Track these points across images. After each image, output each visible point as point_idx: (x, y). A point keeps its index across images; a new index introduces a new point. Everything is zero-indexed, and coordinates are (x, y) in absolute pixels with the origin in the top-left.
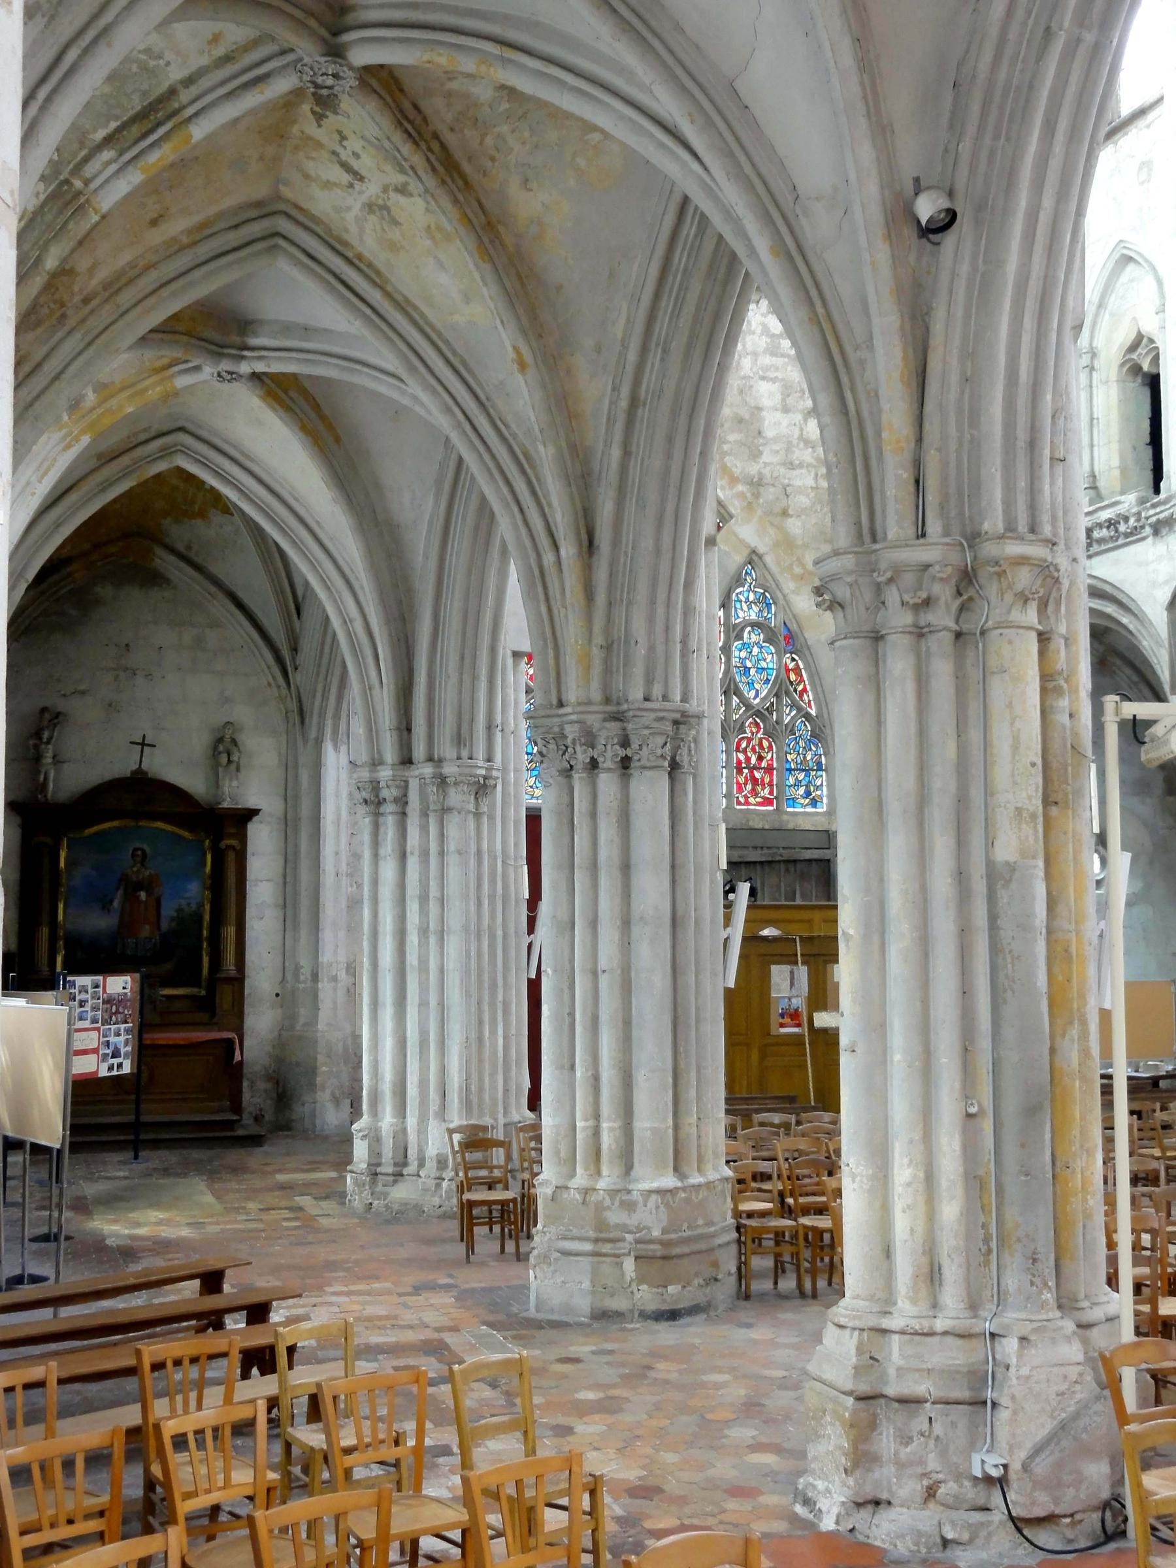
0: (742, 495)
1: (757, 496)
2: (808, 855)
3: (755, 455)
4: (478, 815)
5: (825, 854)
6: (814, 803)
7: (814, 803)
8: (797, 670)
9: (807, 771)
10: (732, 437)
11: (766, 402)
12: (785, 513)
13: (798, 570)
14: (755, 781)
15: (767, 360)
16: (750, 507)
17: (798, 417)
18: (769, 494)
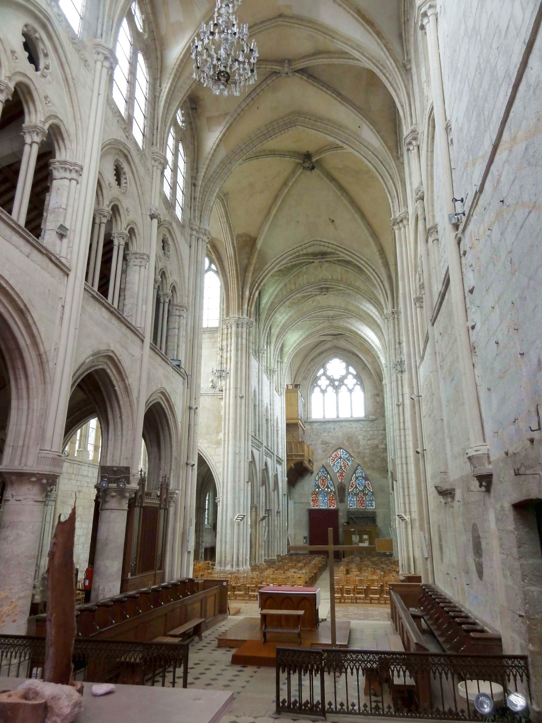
3: (358, 448)
11: (360, 439)
12: (364, 457)
15: (360, 432)
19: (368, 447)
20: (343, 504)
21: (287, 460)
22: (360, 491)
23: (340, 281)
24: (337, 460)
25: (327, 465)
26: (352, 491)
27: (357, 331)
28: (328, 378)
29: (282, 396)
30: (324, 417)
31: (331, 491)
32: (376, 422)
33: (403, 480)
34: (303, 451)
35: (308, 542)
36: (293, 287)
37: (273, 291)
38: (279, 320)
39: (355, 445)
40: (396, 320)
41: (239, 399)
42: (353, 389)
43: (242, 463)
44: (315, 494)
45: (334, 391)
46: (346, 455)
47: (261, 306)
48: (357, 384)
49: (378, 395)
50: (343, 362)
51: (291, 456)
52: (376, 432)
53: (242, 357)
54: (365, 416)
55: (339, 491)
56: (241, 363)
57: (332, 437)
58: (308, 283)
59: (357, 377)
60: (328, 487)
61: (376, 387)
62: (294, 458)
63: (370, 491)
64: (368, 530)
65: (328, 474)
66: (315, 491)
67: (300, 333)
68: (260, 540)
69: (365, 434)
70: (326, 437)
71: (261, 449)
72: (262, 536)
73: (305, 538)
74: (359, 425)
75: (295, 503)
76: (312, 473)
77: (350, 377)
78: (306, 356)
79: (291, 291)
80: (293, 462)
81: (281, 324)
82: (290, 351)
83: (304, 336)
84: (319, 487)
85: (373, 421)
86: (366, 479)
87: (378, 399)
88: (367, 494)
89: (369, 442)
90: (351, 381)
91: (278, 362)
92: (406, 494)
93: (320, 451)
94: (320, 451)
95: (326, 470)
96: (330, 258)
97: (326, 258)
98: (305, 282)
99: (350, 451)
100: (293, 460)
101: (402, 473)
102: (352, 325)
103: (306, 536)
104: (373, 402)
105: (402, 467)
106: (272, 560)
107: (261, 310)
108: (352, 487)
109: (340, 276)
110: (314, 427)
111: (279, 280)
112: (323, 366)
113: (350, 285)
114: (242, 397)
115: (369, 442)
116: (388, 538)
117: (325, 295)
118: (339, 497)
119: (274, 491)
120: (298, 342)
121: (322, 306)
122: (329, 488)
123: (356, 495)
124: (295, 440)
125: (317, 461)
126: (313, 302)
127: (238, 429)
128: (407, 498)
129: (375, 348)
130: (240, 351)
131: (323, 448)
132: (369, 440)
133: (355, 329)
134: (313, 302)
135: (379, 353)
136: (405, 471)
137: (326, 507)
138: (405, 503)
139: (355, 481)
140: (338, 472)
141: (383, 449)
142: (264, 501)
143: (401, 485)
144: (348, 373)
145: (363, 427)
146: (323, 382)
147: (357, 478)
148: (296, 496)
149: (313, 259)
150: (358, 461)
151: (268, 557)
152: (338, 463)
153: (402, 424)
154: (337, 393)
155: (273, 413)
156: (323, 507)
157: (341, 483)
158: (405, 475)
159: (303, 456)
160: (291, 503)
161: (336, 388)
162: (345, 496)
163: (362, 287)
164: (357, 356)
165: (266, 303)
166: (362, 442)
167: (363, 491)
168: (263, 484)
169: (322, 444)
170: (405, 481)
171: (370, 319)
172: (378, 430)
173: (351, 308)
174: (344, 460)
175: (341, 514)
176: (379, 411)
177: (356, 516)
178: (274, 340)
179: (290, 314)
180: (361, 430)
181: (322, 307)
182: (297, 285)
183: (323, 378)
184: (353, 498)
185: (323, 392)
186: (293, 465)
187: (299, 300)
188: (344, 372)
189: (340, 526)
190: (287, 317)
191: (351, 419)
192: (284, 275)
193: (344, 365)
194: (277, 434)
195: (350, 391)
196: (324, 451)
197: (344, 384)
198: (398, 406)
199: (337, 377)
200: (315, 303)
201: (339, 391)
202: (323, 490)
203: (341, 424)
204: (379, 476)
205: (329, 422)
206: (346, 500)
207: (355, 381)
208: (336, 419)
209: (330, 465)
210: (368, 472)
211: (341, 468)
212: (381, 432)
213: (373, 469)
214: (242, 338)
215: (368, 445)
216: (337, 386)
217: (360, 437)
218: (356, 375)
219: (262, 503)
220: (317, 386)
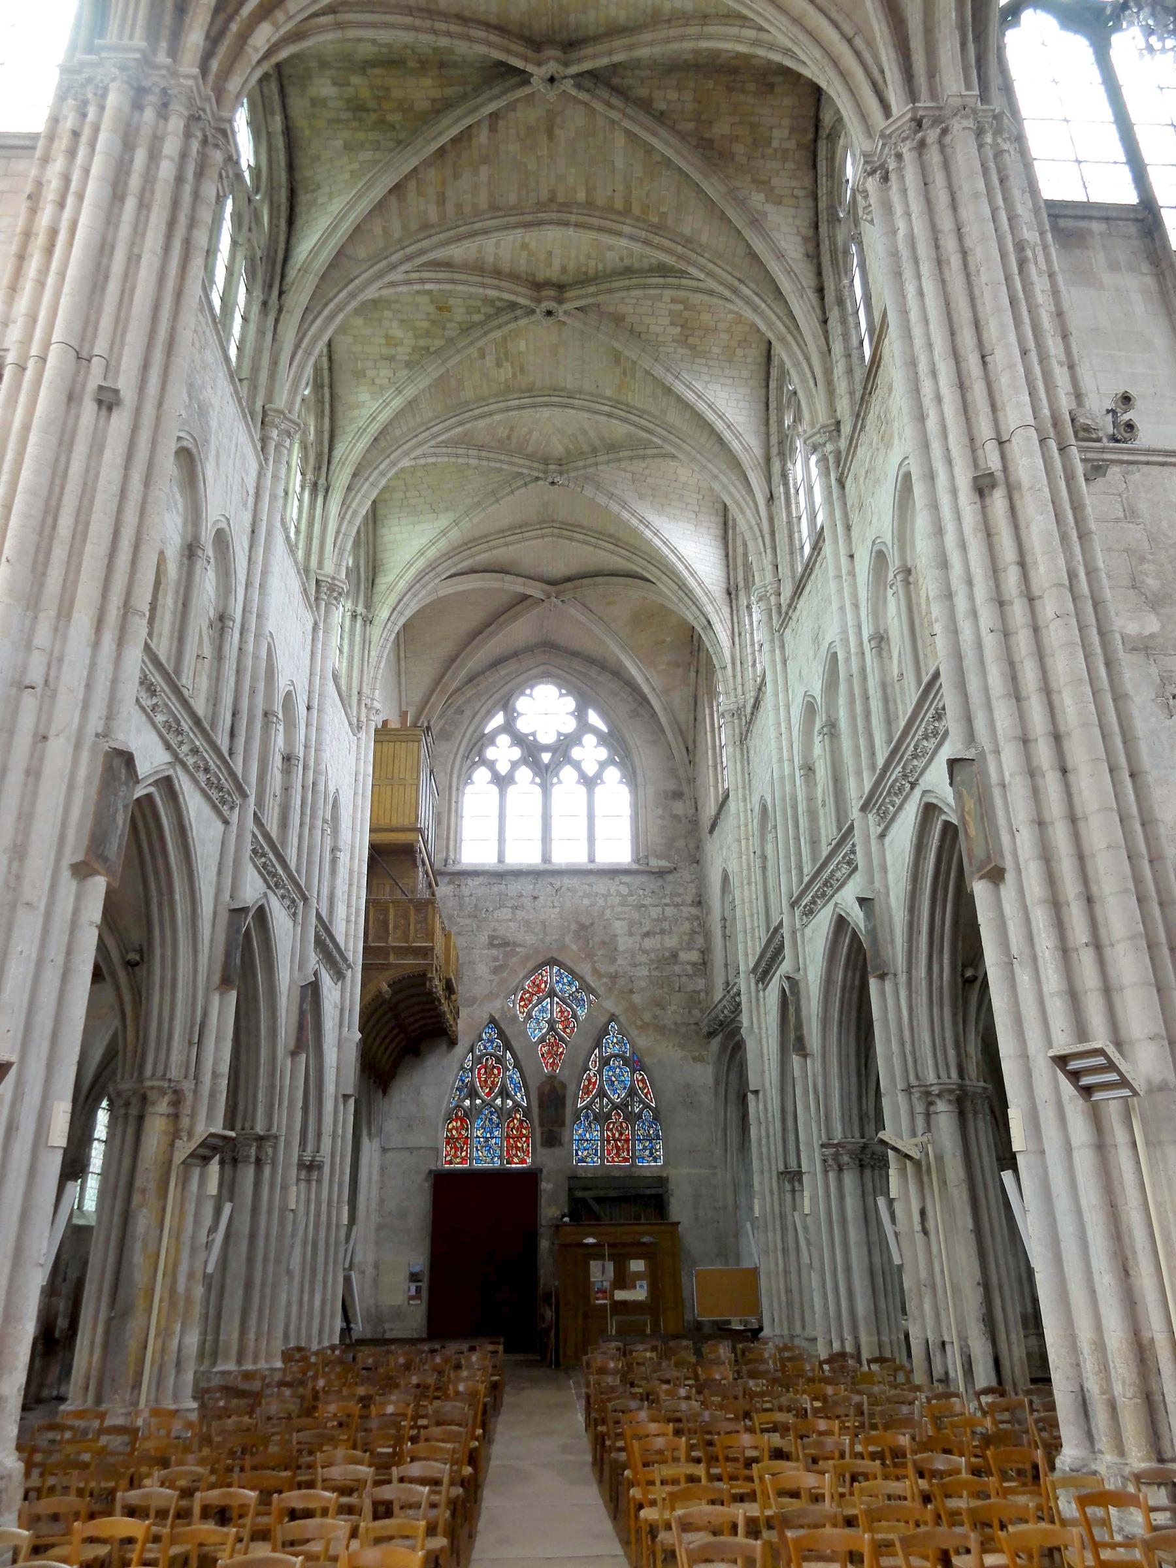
0: (606, 984)
1: (614, 983)
2: (648, 1192)
3: (613, 960)
4: (308, 1181)
5: (660, 1191)
6: (655, 1160)
7: (655, 1160)
8: (643, 1081)
9: (650, 1141)
10: (599, 953)
11: (619, 932)
12: (631, 992)
13: (639, 1023)
14: (618, 1148)
15: (620, 909)
16: (610, 990)
17: (638, 938)
18: (621, 982)
19: (643, 959)
20: (557, 1151)
21: (365, 967)
22: (616, 1107)
23: (619, 213)
24: (540, 1001)
25: (503, 1012)
26: (586, 1107)
27: (642, 527)
28: (519, 740)
29: (363, 735)
30: (501, 860)
31: (517, 1105)
32: (670, 878)
33: (1047, 857)
34: (430, 935)
35: (425, 1293)
36: (433, 214)
37: (351, 206)
38: (365, 412)
39: (599, 953)
40: (934, 156)
41: (89, 408)
42: (599, 776)
43: (58, 751)
44: (457, 1118)
45: (538, 780)
46: (570, 984)
47: (292, 262)
48: (610, 762)
49: (678, 795)
50: (569, 693)
51: (384, 952)
52: (670, 911)
53: (139, 231)
54: (637, 860)
55: (541, 1106)
56: (133, 259)
57: (527, 923)
58: (493, 207)
59: (614, 740)
60: (504, 1094)
61: (673, 772)
62: (392, 959)
63: (648, 1107)
64: (645, 1239)
65: (508, 1046)
66: (458, 1106)
67: (443, 521)
68: (183, 1269)
69: (635, 915)
70: (505, 923)
71: (234, 818)
72: (194, 1250)
73: (414, 1277)
74: (613, 886)
75: (384, 1150)
76: (453, 1043)
77: (589, 740)
78: (453, 660)
79: (425, 226)
80: (390, 975)
81: (375, 428)
82: (402, 585)
83: (455, 534)
84: (473, 1094)
85: (661, 874)
86: (635, 1063)
87: (679, 808)
88: (639, 1116)
89: (648, 943)
90: (590, 752)
91: (354, 617)
92: (1079, 933)
93: (482, 969)
94: (482, 969)
95: (502, 1034)
96: (594, 56)
97: (580, 60)
98: (483, 201)
99: (584, 969)
100: (388, 966)
101: (1041, 824)
102: (624, 505)
103: (416, 1269)
104: (662, 817)
105: (1036, 794)
106: (248, 1376)
107: (292, 273)
108: (588, 1092)
109: (620, 188)
110: (466, 891)
111: (377, 162)
112: (506, 704)
113: (659, 229)
114: (108, 401)
115: (648, 943)
116: (746, 1264)
117: (549, 313)
118: (541, 1125)
119: (294, 1054)
120: (432, 553)
121: (530, 390)
122: (508, 1096)
123: (602, 1118)
124: (399, 896)
125: (472, 1001)
126: (499, 364)
127: (59, 554)
128: (1086, 961)
129: (698, 592)
130: (130, 204)
131: (495, 959)
132: (647, 934)
133: (634, 522)
134: (499, 364)
135: (709, 609)
136: (1055, 807)
137: (497, 1164)
138: (1074, 997)
139: (600, 1071)
140: (542, 1040)
141: (694, 964)
142: (225, 1068)
143: (1035, 888)
144: (584, 726)
145: (631, 894)
146: (503, 752)
147: (605, 1062)
148: (391, 1126)
149: (526, 59)
150: (610, 1005)
151: (239, 1361)
152: (543, 1010)
153: (1012, 577)
154: (546, 789)
155: (319, 742)
156: (484, 1160)
157: (551, 1078)
158: (1060, 835)
159: (426, 952)
160: (370, 1149)
161: (545, 774)
162: (563, 1124)
163: (704, 239)
164: (617, 673)
165: (315, 252)
166: (625, 943)
167: (623, 1106)
168: (226, 982)
169: (491, 945)
170: (1066, 867)
171: (703, 440)
172: (677, 905)
173: (638, 397)
174: (563, 1000)
175: (546, 1186)
176: (680, 844)
177: (601, 1193)
178: (341, 479)
179: (410, 392)
180: (623, 904)
181: (530, 390)
182: (450, 208)
183: (504, 740)
184: (589, 1129)
185: (502, 782)
186: (385, 987)
187: (451, 341)
188: (570, 725)
189: (542, 1230)
190: (398, 403)
191: (591, 866)
192: (399, 142)
193: (570, 703)
194: (334, 860)
195: (590, 783)
196: (496, 971)
197: (569, 760)
198: (983, 486)
199: (547, 737)
200: (504, 373)
201: (555, 780)
202: (490, 1105)
203: (557, 882)
204: (680, 1053)
205: (518, 874)
206: (566, 1139)
207: (603, 753)
208: (543, 867)
209: (516, 1017)
210: (642, 1042)
211: (552, 1028)
212: (687, 911)
213: (661, 1030)
214: (154, 156)
215: (645, 952)
216: (547, 767)
217: (619, 927)
218: (611, 733)
219: (215, 1075)
220: (484, 762)
